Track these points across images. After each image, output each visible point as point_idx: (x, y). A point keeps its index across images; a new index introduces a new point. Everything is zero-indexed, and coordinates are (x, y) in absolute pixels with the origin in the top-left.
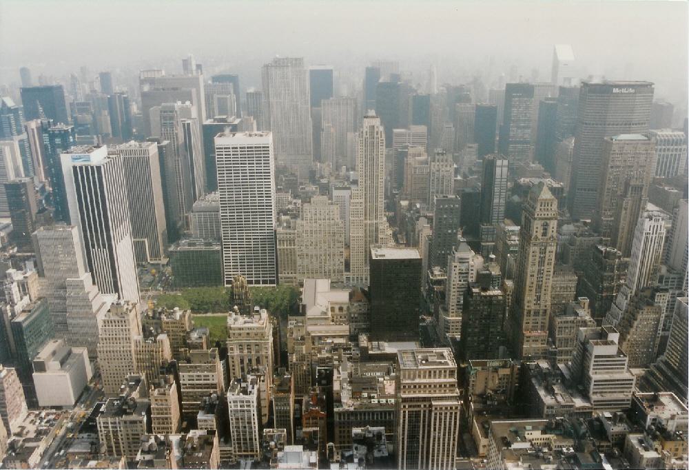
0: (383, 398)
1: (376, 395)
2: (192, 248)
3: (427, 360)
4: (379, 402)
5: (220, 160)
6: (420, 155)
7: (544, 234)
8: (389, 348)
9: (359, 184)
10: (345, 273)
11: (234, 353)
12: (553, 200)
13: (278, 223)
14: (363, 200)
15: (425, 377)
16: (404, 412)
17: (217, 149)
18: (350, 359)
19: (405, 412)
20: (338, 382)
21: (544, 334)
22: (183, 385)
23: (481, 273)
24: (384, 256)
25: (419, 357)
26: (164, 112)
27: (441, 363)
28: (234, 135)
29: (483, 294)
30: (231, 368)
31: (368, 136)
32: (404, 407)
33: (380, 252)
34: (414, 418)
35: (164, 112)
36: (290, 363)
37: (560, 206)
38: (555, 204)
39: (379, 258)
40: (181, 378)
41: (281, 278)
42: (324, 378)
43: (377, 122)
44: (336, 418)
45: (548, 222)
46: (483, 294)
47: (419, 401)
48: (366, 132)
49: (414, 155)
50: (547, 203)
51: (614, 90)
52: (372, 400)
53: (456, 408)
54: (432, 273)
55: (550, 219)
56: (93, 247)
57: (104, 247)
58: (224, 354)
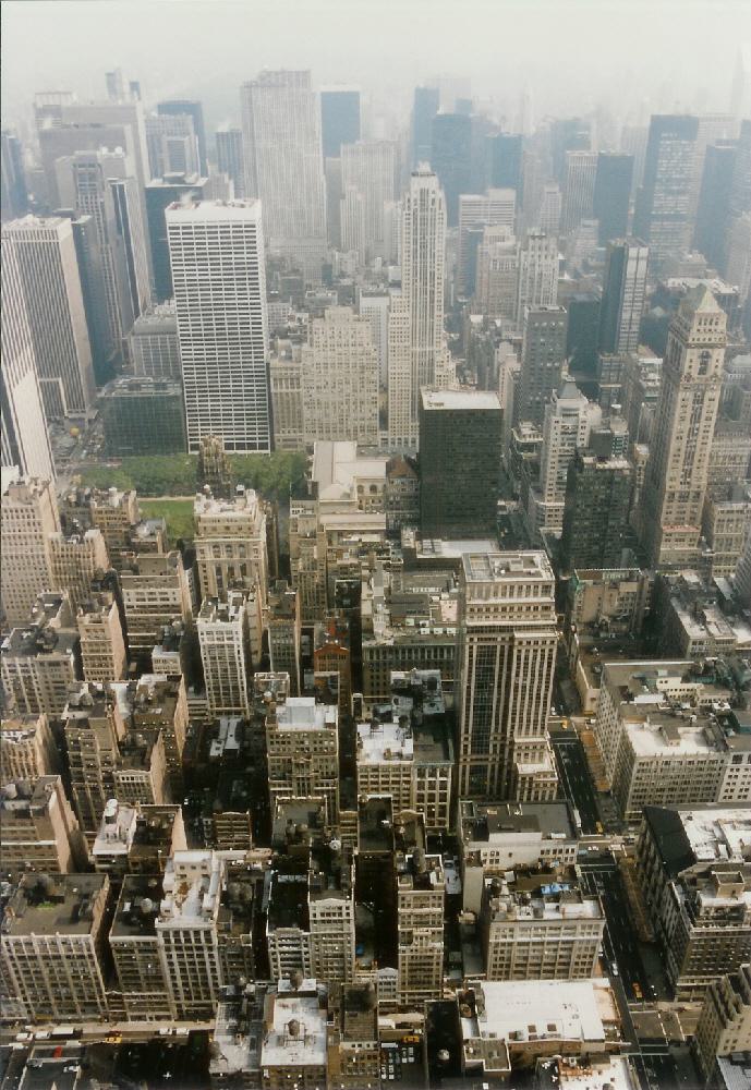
0: (437, 626)
1: (427, 622)
2: (135, 394)
3: (508, 570)
4: (432, 632)
7: (702, 371)
8: (448, 549)
9: (403, 286)
10: (379, 432)
11: (207, 556)
12: (719, 314)
13: (272, 352)
15: (504, 595)
16: (471, 648)
17: (170, 228)
18: (387, 567)
19: (472, 647)
20: (369, 603)
21: (692, 530)
22: (128, 607)
23: (597, 432)
24: (442, 404)
25: (497, 564)
27: (529, 574)
28: (197, 205)
29: (600, 466)
30: (202, 581)
32: (471, 639)
34: (486, 656)
36: (293, 574)
37: (730, 327)
38: (724, 319)
39: (434, 408)
40: (125, 597)
42: (346, 596)
43: (432, 183)
44: (366, 657)
46: (600, 466)
47: (494, 631)
48: (415, 200)
50: (711, 320)
52: (422, 630)
53: (552, 642)
54: (519, 432)
55: (712, 346)
58: (190, 560)
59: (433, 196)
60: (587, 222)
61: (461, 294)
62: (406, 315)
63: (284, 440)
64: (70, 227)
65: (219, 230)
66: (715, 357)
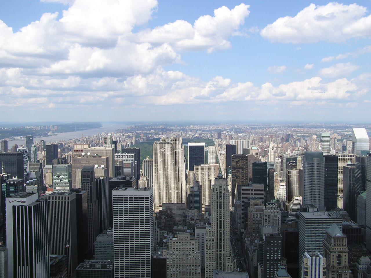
6: (258, 205)
13: (154, 252)
17: (114, 198)
28: (127, 188)
31: (218, 191)
45: (341, 254)
49: (254, 205)
55: (342, 252)
56: (19, 265)
57: (27, 265)
60: (296, 197)
61: (242, 228)
65: (134, 199)
66: (344, 257)
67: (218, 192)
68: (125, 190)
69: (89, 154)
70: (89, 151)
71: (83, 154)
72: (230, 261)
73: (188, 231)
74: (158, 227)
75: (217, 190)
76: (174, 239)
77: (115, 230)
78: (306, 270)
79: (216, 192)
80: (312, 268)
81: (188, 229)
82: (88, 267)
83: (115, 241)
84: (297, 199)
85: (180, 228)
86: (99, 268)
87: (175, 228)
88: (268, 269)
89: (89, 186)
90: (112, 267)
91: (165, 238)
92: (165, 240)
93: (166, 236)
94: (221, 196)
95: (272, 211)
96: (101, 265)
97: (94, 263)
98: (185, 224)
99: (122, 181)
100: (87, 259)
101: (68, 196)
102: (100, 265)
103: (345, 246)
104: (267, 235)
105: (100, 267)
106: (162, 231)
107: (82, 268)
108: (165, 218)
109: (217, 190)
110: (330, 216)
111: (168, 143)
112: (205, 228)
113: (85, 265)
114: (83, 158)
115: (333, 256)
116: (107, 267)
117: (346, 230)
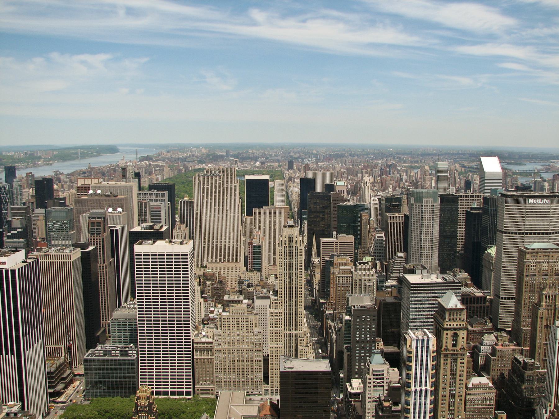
5: (140, 267)
6: (346, 264)
7: (454, 345)
14: (282, 310)
17: (137, 255)
23: (392, 385)
24: (292, 368)
26: (93, 218)
28: (154, 242)
29: (394, 408)
31: (287, 245)
33: (289, 364)
35: (93, 218)
37: (469, 316)
38: (465, 313)
39: (287, 370)
41: (198, 390)
43: (296, 231)
48: (285, 241)
49: (340, 264)
51: (530, 200)
54: (351, 385)
55: (460, 329)
59: (296, 239)
60: (399, 254)
62: (280, 311)
63: (201, 390)
64: (80, 253)
67: (288, 247)
68: (153, 243)
69: (99, 192)
70: (99, 188)
71: (91, 192)
72: (305, 344)
73: (246, 301)
74: (202, 297)
75: (285, 244)
76: (225, 314)
77: (138, 302)
78: (408, 355)
79: (284, 247)
80: (417, 352)
81: (245, 299)
82: (102, 354)
83: (139, 317)
84: (401, 257)
85: (234, 297)
86: (117, 356)
87: (226, 297)
88: (357, 355)
89: (100, 239)
90: (136, 355)
91: (212, 312)
92: (211, 315)
93: (212, 309)
94: (291, 252)
95: (364, 273)
96: (121, 351)
97: (110, 349)
98: (241, 292)
99: (148, 230)
100: (100, 344)
101: (69, 254)
102: (119, 352)
103: (463, 321)
104: (356, 308)
105: (119, 354)
106: (206, 303)
107: (92, 356)
108: (212, 284)
109: (285, 244)
110: (446, 280)
111: (216, 175)
112: (269, 298)
113: (96, 352)
114: (91, 198)
115: (447, 334)
116: (129, 355)
117: (465, 299)
